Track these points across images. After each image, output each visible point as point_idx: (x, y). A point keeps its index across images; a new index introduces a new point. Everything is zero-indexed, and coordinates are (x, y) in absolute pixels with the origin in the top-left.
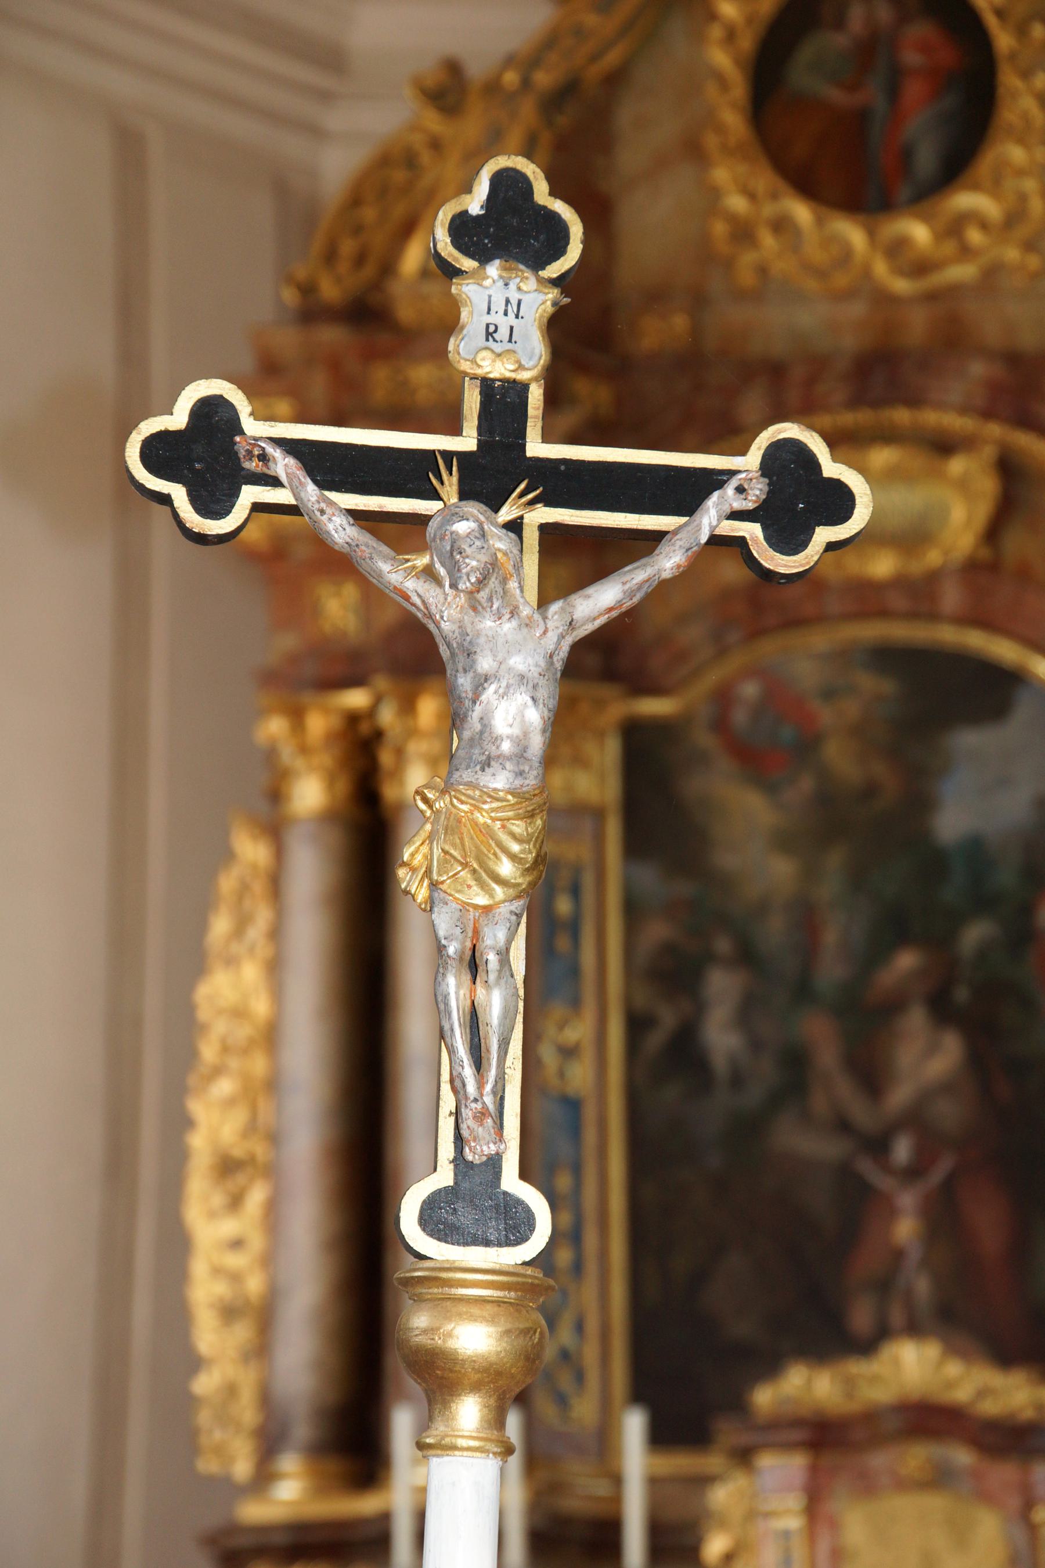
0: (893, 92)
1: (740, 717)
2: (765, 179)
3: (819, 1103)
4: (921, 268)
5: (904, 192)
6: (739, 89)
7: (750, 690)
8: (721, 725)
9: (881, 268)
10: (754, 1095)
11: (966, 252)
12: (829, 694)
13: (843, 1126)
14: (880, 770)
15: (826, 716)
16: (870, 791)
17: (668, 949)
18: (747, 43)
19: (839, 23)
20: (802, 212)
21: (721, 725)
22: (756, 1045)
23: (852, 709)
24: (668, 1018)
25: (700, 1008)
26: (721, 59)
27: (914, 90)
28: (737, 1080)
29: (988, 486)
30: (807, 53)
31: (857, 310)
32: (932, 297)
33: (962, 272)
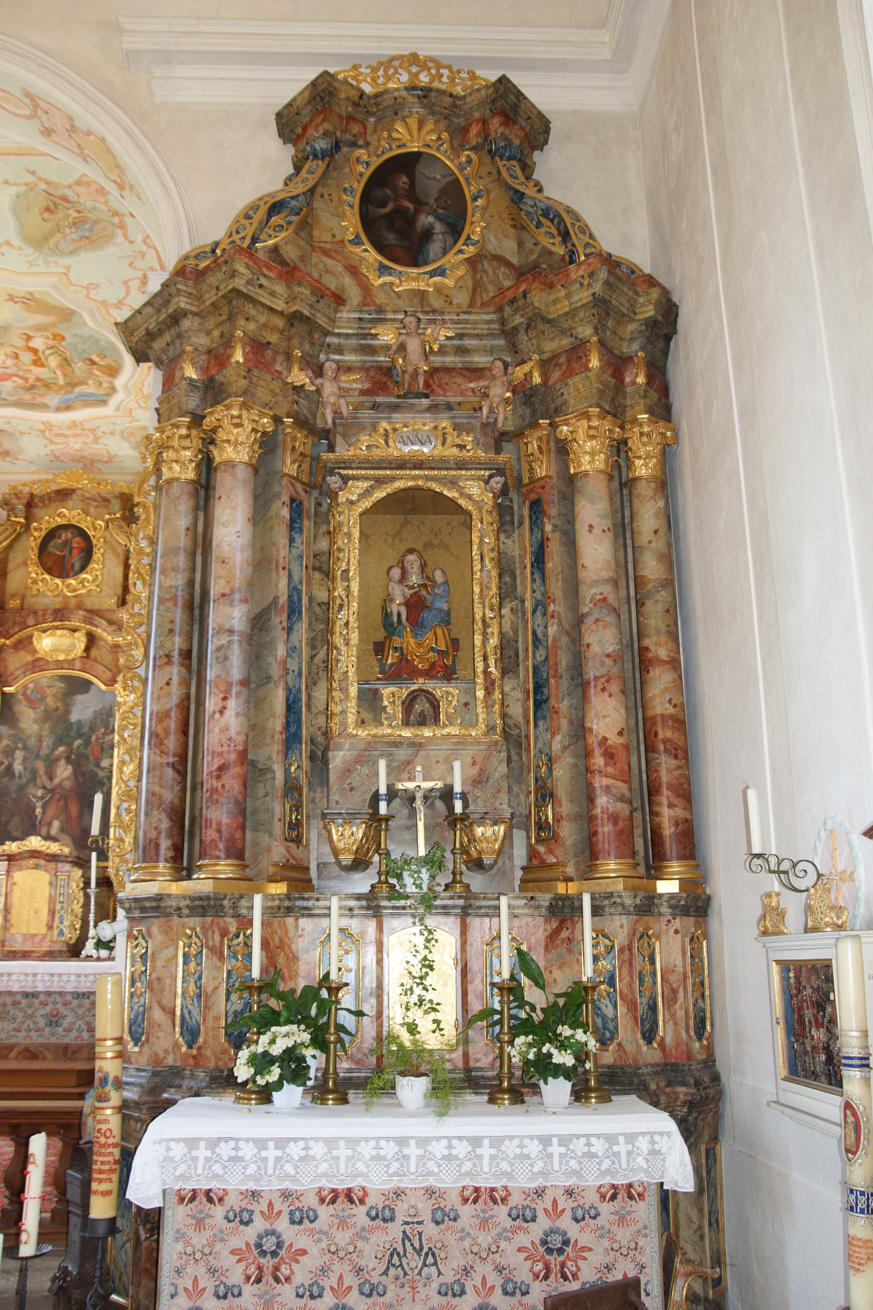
0: (71, 552)
1: (29, 692)
2: (40, 570)
3: (39, 782)
4: (74, 590)
5: (72, 574)
6: (36, 551)
7: (31, 686)
8: (24, 694)
9: (65, 590)
10: (24, 780)
11: (84, 586)
12: (49, 687)
13: (44, 788)
14: (59, 704)
15: (48, 692)
16: (57, 709)
17: (8, 746)
18: (39, 541)
19: (60, 538)
20: (47, 577)
21: (24, 694)
22: (25, 769)
23: (54, 690)
24: (6, 763)
25: (14, 760)
26: (33, 544)
27: (75, 552)
28: (20, 777)
29: (84, 639)
30: (52, 543)
31: (60, 599)
32: (75, 596)
33: (84, 591)
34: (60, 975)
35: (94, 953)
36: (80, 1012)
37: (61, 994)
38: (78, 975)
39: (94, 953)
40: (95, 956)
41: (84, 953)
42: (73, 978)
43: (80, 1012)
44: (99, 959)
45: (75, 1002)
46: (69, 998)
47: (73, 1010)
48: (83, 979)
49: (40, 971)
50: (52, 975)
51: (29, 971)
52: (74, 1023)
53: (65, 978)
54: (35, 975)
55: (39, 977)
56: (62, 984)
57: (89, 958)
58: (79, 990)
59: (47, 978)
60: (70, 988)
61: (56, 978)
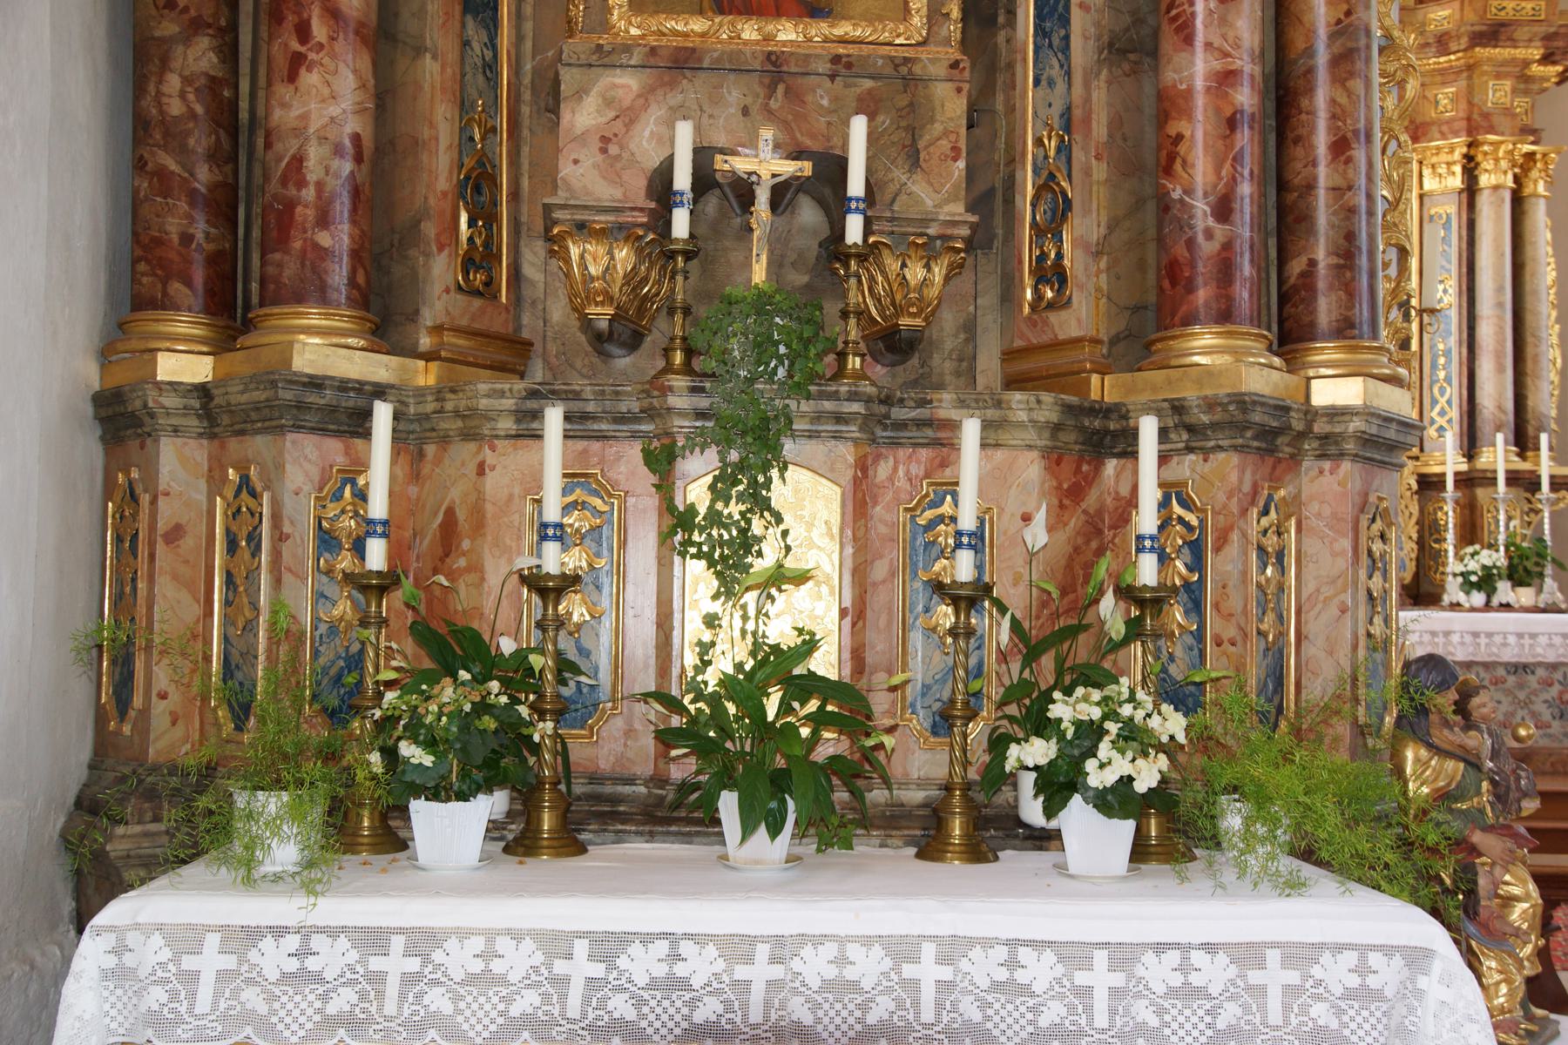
34: (1489, 635)
35: (1461, 597)
36: (1522, 695)
37: (1487, 666)
38: (1520, 636)
39: (1461, 597)
40: (1467, 605)
41: (1446, 599)
42: (1512, 640)
43: (1522, 695)
44: (1473, 609)
45: (1512, 680)
46: (1501, 672)
47: (1508, 692)
48: (1527, 641)
49: (1456, 627)
50: (1476, 635)
51: (1437, 627)
52: (1513, 714)
53: (1498, 639)
54: (1447, 634)
55: (1455, 638)
56: (1495, 650)
57: (1456, 606)
58: (1523, 660)
59: (1468, 639)
60: (1508, 656)
61: (1483, 640)
